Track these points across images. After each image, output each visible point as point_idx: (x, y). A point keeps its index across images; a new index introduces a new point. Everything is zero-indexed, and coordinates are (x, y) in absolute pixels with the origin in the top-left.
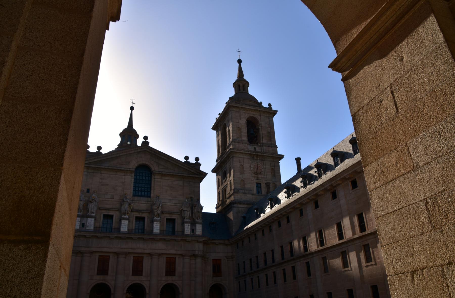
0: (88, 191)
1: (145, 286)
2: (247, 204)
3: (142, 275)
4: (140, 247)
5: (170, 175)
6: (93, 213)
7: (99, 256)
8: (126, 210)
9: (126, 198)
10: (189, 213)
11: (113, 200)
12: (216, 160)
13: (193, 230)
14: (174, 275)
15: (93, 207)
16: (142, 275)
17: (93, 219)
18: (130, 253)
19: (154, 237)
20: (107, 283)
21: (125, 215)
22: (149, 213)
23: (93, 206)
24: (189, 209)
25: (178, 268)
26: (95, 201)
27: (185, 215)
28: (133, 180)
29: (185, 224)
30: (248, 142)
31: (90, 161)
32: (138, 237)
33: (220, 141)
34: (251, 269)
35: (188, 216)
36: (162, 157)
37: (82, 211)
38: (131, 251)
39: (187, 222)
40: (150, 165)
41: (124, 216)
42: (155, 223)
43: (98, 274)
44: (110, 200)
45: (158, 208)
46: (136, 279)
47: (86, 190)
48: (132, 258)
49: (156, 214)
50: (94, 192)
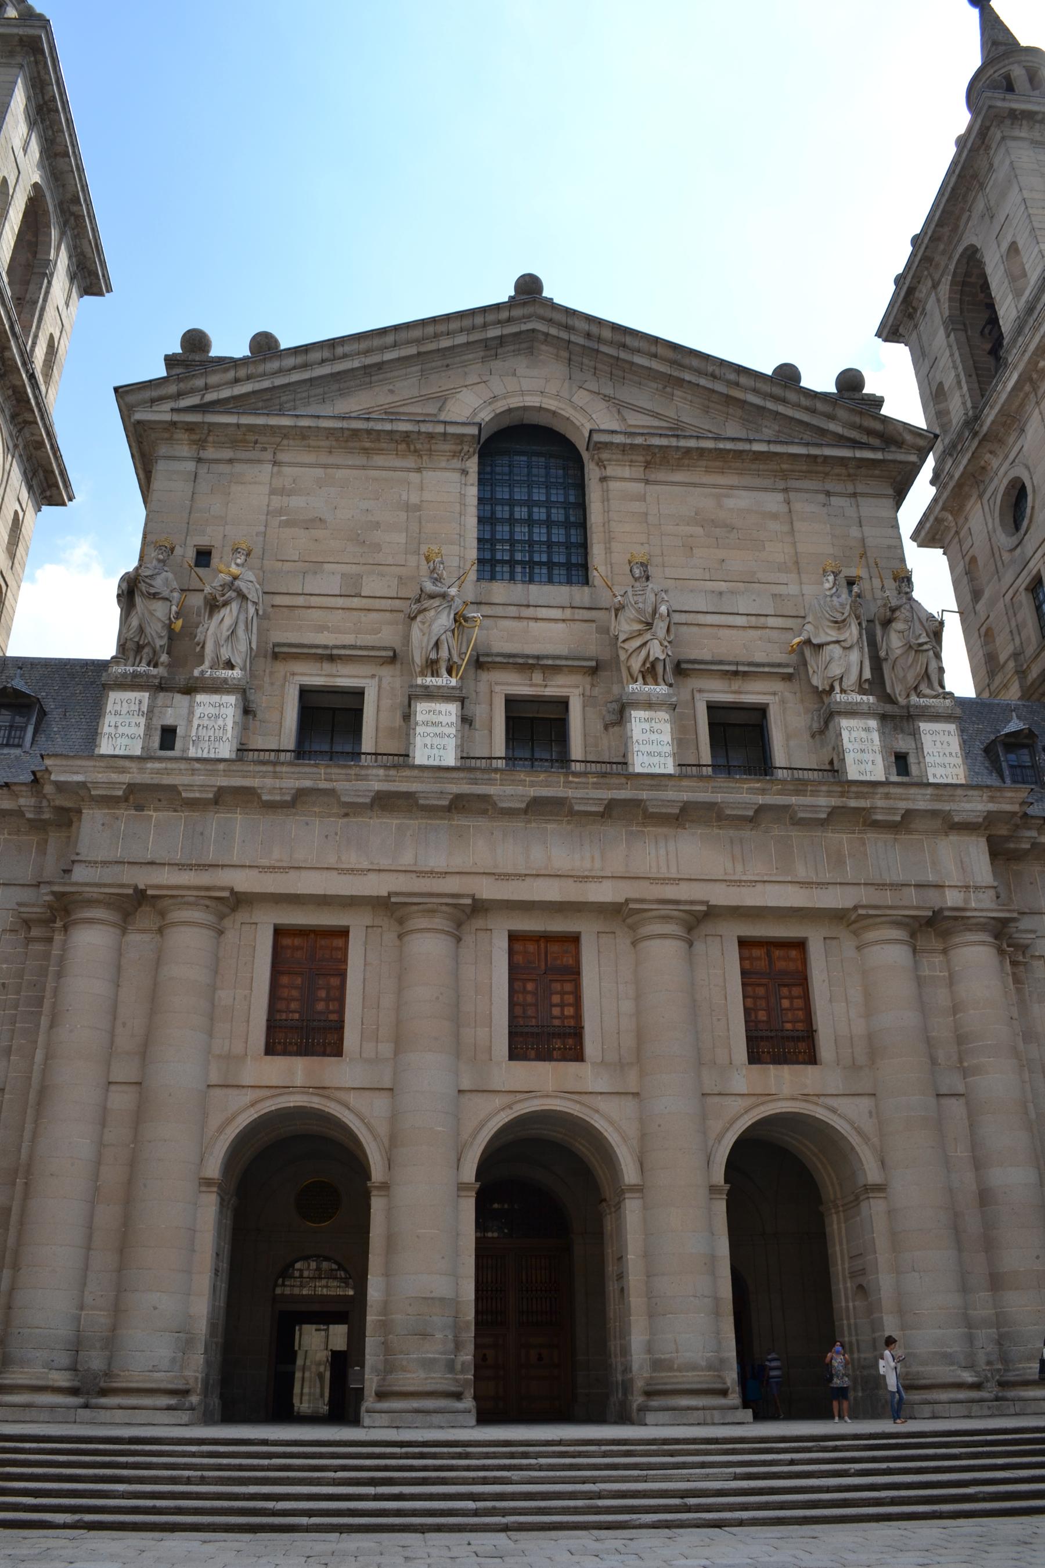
0: (203, 557)
1: (612, 1136)
3: (578, 1056)
4: (547, 865)
5: (702, 452)
6: (229, 665)
7: (279, 932)
8: (437, 645)
9: (437, 580)
10: (854, 656)
11: (356, 602)
13: (901, 762)
14: (812, 1059)
15: (226, 636)
16: (578, 1056)
17: (231, 699)
18: (479, 908)
19: (644, 795)
20: (333, 1108)
21: (435, 673)
22: (595, 670)
23: (228, 622)
24: (852, 632)
25: (834, 1010)
26: (243, 597)
27: (836, 670)
28: (472, 492)
29: (845, 723)
31: (210, 397)
32: (533, 792)
33: (945, 360)
35: (852, 679)
36: (638, 360)
37: (164, 658)
38: (489, 890)
39: (852, 712)
40: (568, 412)
42: (636, 714)
43: (270, 1050)
44: (340, 602)
45: (649, 625)
46: (543, 1086)
47: (191, 554)
48: (501, 944)
49: (636, 664)
50: (236, 550)
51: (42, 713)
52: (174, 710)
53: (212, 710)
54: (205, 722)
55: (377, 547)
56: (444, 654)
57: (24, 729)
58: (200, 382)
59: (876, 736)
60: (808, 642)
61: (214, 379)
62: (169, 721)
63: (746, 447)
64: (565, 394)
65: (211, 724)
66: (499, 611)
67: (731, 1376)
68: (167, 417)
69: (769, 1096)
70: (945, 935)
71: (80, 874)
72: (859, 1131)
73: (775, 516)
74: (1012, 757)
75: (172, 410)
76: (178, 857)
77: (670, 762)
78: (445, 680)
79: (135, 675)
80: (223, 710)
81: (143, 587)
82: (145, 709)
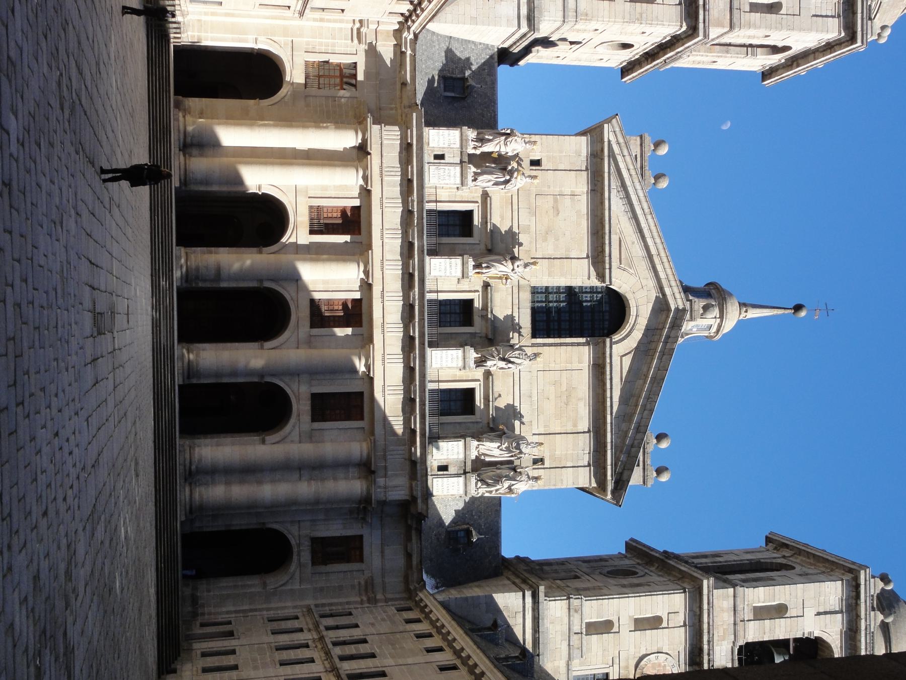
2: (536, 642)
3: (312, 326)
5: (604, 391)
6: (475, 180)
8: (488, 267)
9: (526, 265)
12: (670, 550)
13: (443, 468)
14: (314, 420)
17: (458, 181)
28: (580, 284)
30: (741, 642)
31: (619, 158)
33: (736, 558)
34: (335, 644)
35: (482, 449)
41: (471, 263)
43: (311, 207)
51: (464, 99)
52: (453, 157)
53: (452, 173)
54: (447, 171)
55: (545, 240)
56: (484, 271)
57: (453, 91)
58: (626, 153)
59: (455, 457)
60: (505, 433)
61: (628, 158)
62: (446, 156)
63: (609, 412)
64: (637, 327)
65: (446, 173)
66: (516, 296)
67: (195, 381)
68: (606, 140)
69: (298, 400)
70: (366, 478)
71: (376, 128)
72: (286, 437)
73: (575, 425)
74: (462, 534)
75: (609, 141)
76: (384, 165)
77: (439, 366)
78: (471, 271)
79: (467, 140)
80: (452, 178)
81: (510, 139)
82: (452, 146)
